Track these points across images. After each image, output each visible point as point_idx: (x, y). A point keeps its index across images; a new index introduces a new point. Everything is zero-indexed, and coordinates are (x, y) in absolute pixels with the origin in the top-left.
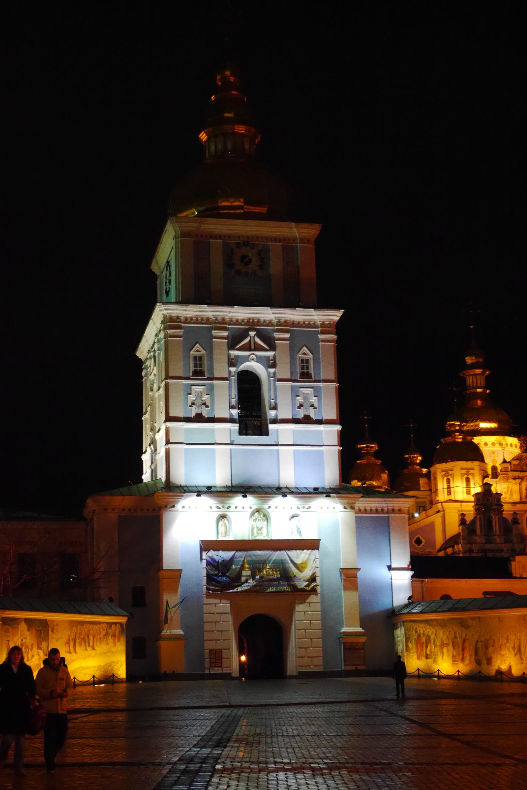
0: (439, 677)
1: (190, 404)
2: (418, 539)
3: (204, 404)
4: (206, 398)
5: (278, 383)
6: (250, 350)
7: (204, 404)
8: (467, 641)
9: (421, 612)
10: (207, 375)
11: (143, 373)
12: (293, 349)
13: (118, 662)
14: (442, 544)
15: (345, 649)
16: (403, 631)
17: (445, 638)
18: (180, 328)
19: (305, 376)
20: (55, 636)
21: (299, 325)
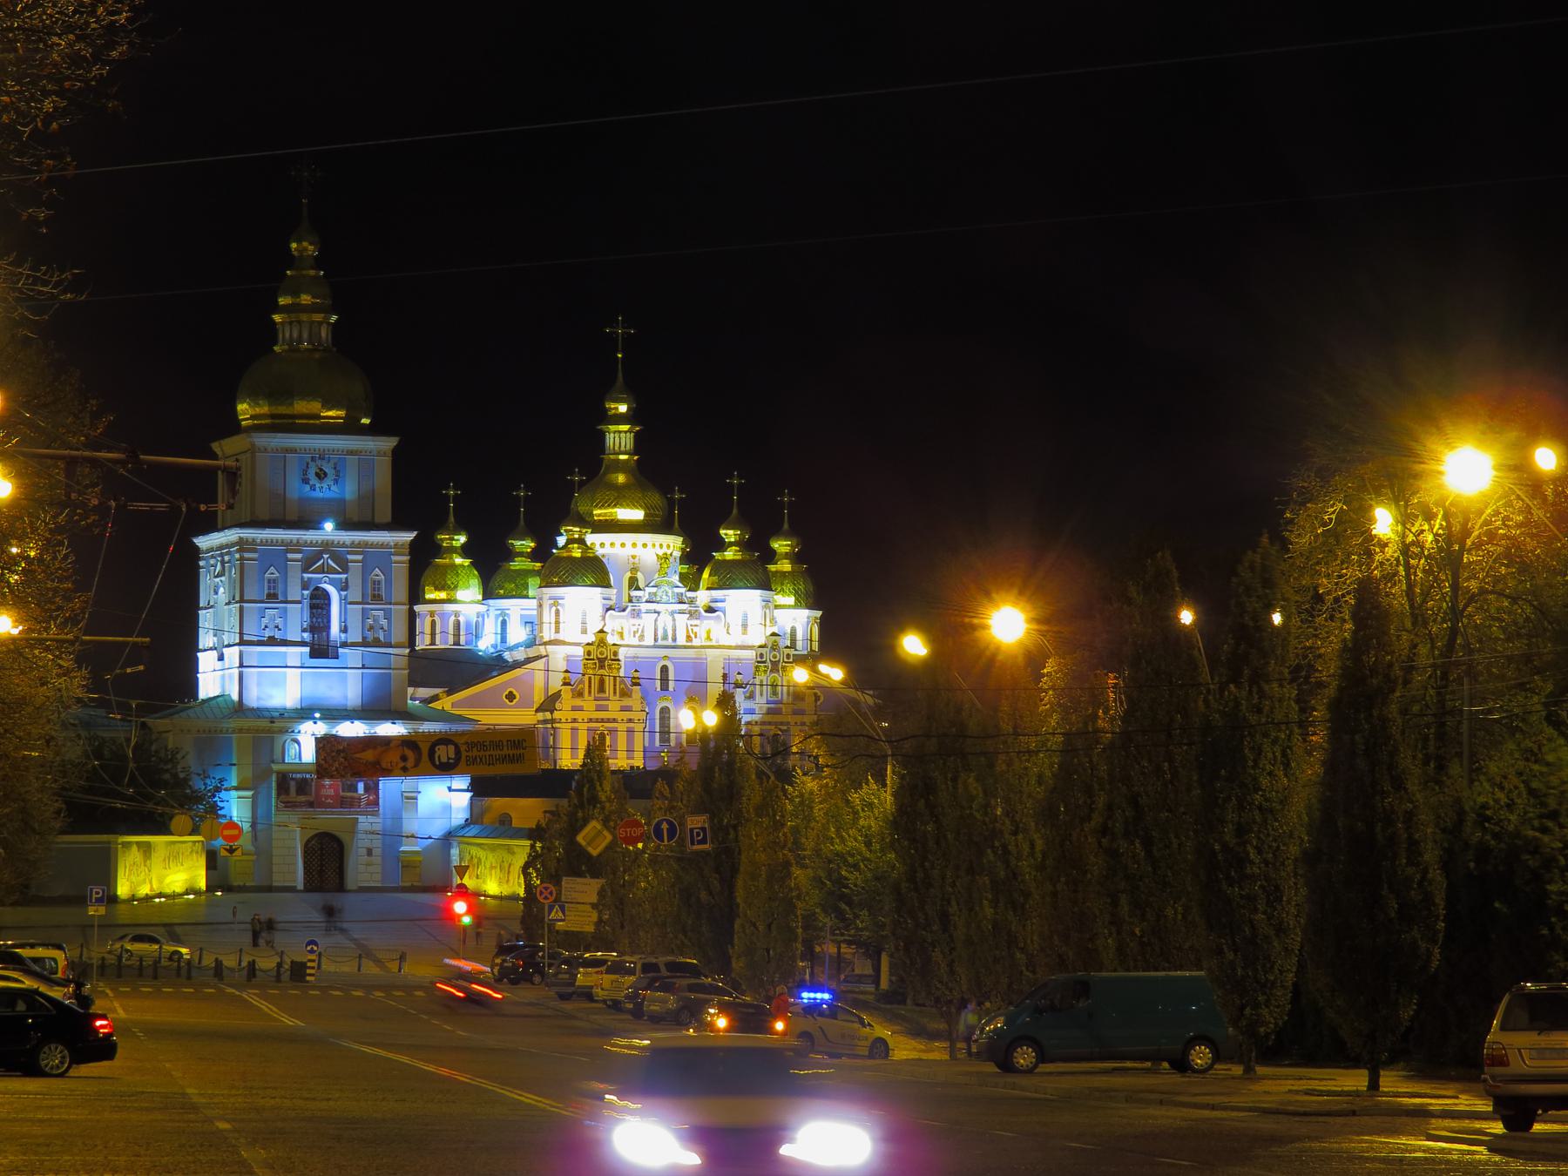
0: (485, 896)
1: (263, 627)
2: (511, 692)
3: (277, 627)
4: (278, 621)
5: (349, 606)
6: (323, 573)
7: (277, 627)
8: (512, 867)
9: (474, 837)
10: (281, 598)
11: (202, 563)
12: (366, 571)
13: (199, 875)
14: (543, 700)
15: (403, 867)
16: (458, 852)
17: (494, 861)
18: (254, 551)
19: (377, 598)
20: (156, 855)
21: (372, 545)
